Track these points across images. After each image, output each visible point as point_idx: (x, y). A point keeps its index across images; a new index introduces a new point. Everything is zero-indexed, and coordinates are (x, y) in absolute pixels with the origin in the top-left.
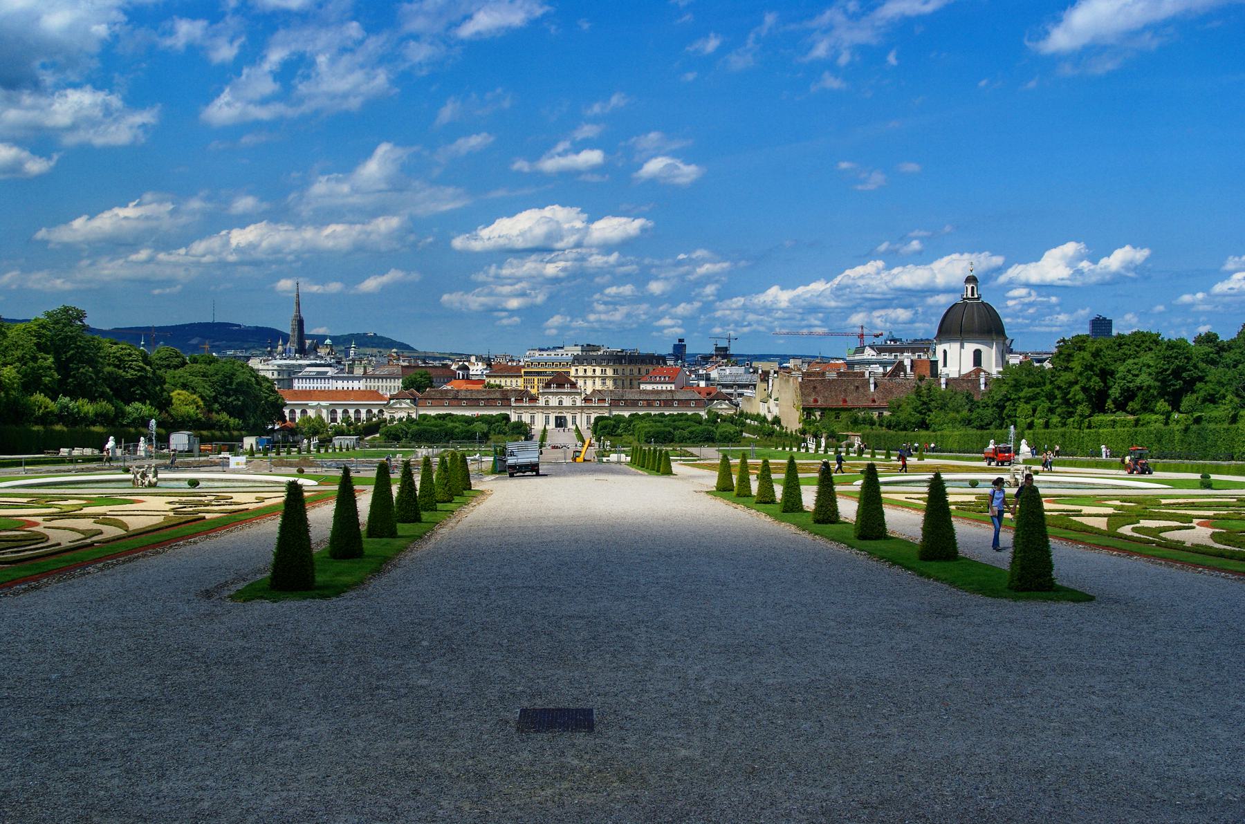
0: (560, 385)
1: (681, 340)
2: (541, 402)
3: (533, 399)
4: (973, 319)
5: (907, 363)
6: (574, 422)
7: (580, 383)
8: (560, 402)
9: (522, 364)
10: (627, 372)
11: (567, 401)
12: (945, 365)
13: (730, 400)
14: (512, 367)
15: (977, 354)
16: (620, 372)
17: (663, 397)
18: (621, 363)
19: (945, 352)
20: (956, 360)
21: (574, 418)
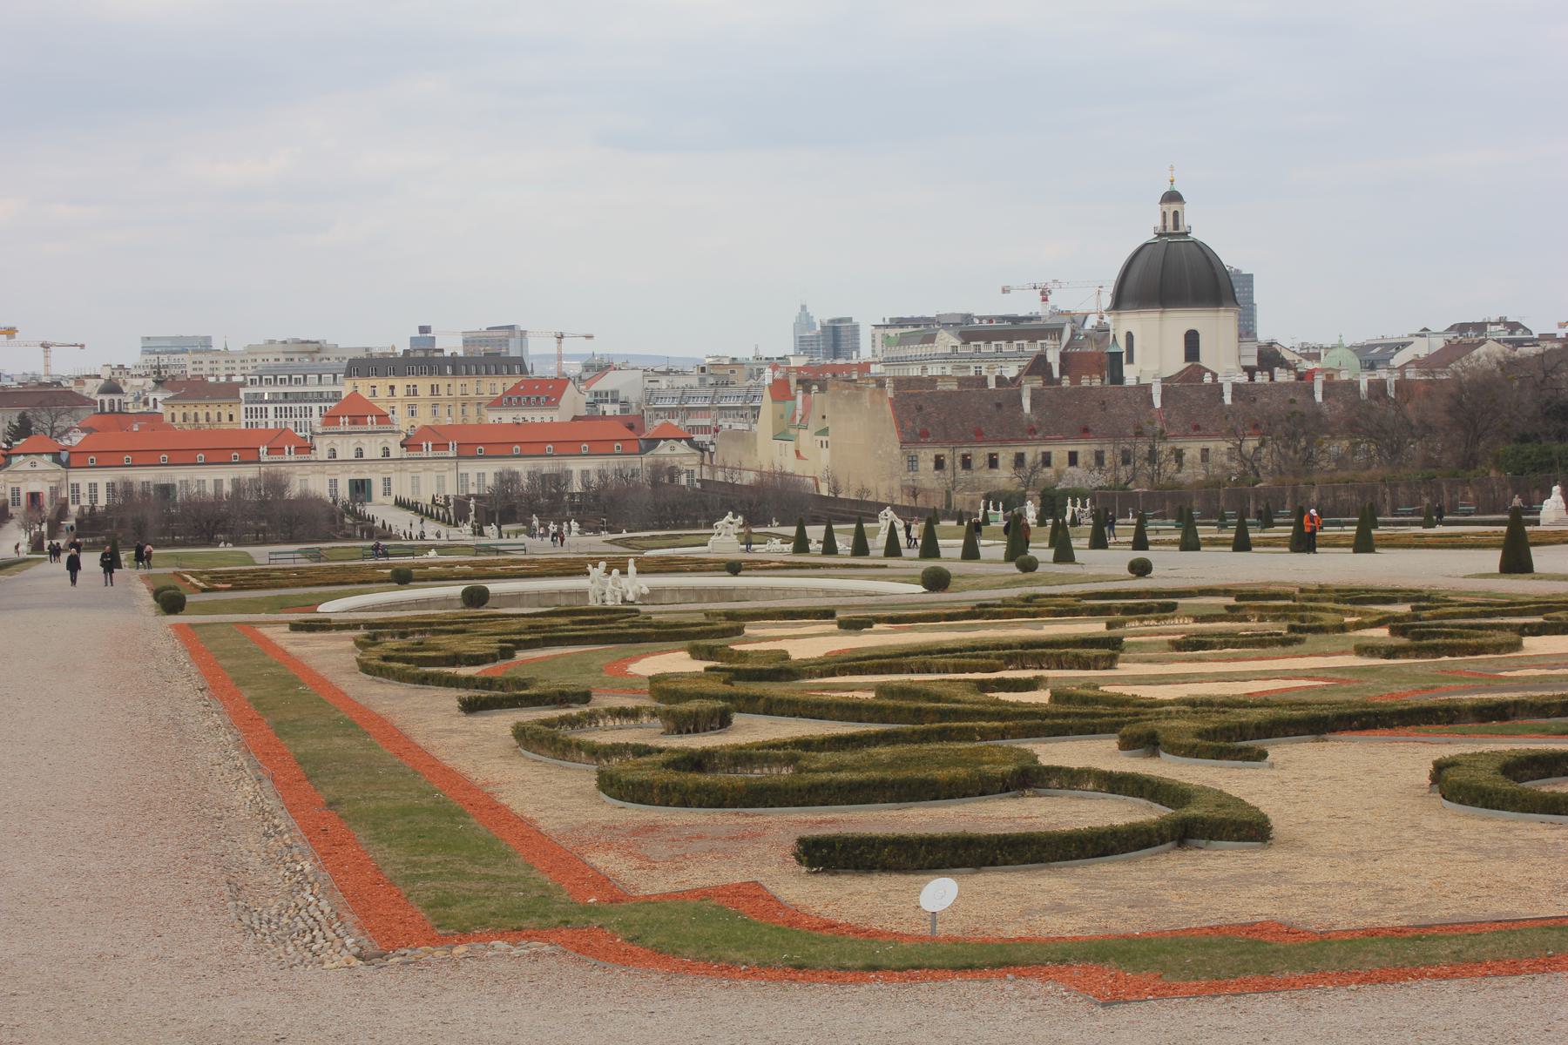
0: (355, 420)
1: (424, 329)
2: (322, 452)
3: (306, 448)
4: (1179, 274)
5: (1053, 358)
6: (387, 492)
8: (360, 453)
9: (237, 379)
11: (373, 448)
12: (1130, 360)
13: (690, 440)
15: (1192, 339)
16: (443, 391)
18: (442, 373)
19: (1130, 336)
20: (1154, 345)
21: (387, 482)
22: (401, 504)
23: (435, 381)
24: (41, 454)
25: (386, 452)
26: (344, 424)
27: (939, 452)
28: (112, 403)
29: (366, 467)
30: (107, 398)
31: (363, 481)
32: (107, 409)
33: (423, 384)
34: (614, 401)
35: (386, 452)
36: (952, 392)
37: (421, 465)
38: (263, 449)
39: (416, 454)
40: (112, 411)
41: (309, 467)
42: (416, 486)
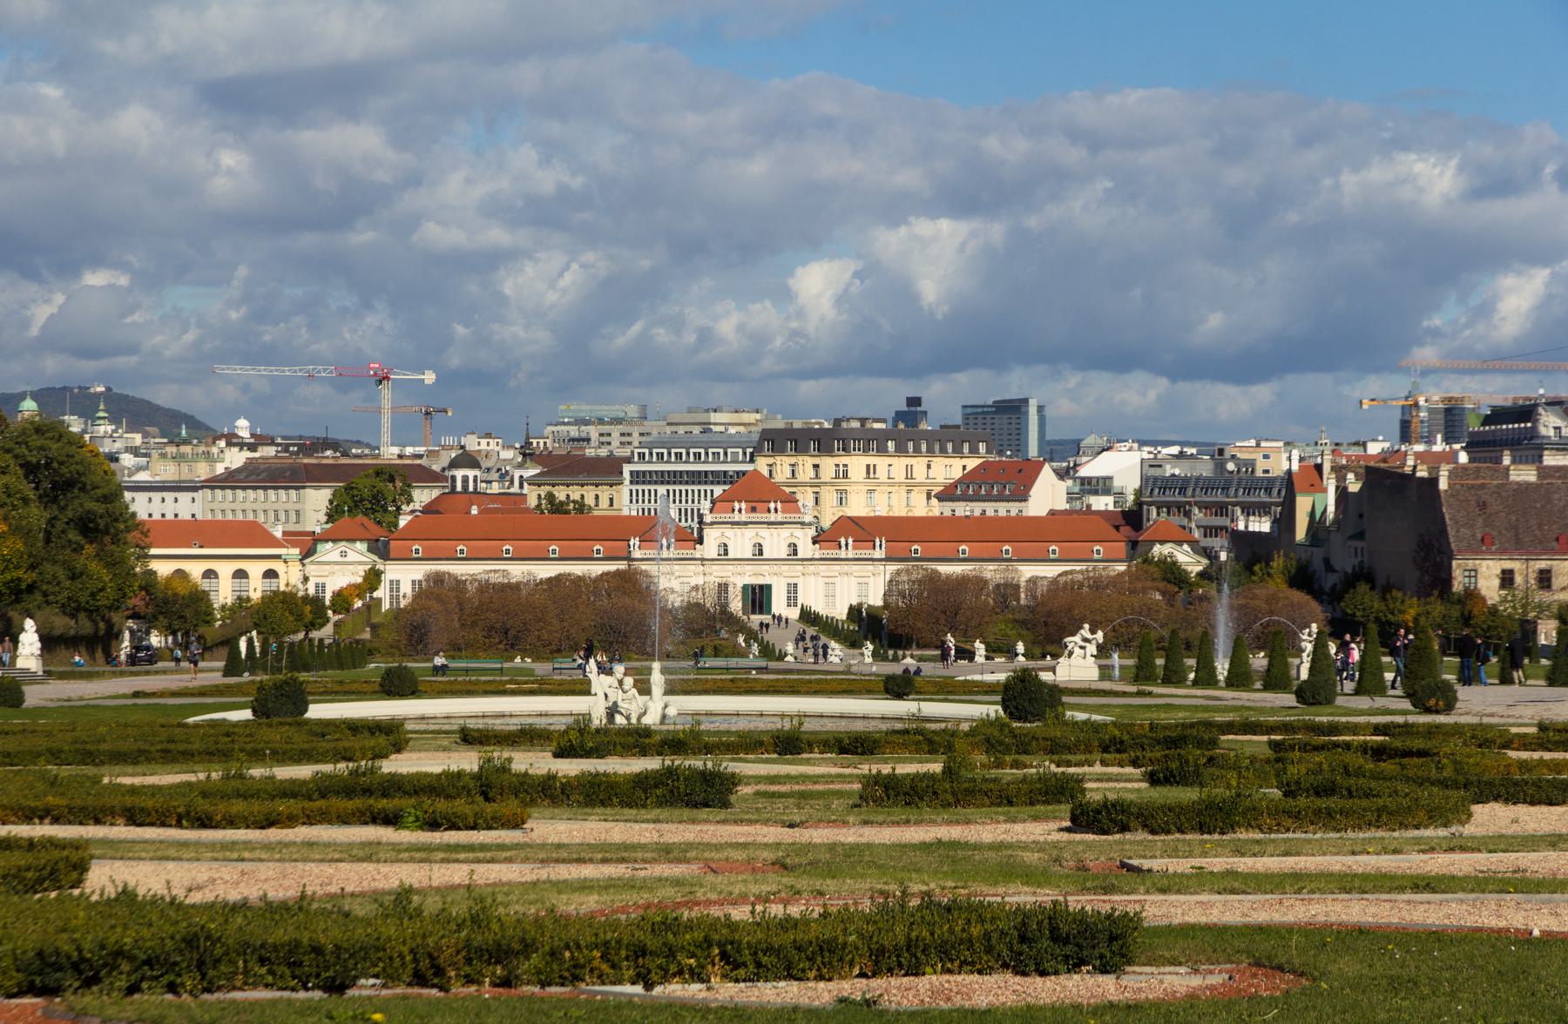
2: (710, 548)
6: (792, 600)
7: (805, 498)
10: (899, 473)
11: (776, 542)
14: (598, 459)
16: (882, 473)
18: (882, 451)
21: (793, 590)
24: (353, 540)
25: (794, 549)
26: (741, 511)
27: (1508, 565)
28: (465, 479)
29: (765, 568)
30: (459, 474)
31: (761, 587)
32: (459, 488)
33: (857, 464)
34: (1107, 491)
35: (794, 549)
36: (1528, 484)
37: (836, 568)
38: (634, 541)
39: (833, 553)
40: (465, 487)
42: (830, 596)
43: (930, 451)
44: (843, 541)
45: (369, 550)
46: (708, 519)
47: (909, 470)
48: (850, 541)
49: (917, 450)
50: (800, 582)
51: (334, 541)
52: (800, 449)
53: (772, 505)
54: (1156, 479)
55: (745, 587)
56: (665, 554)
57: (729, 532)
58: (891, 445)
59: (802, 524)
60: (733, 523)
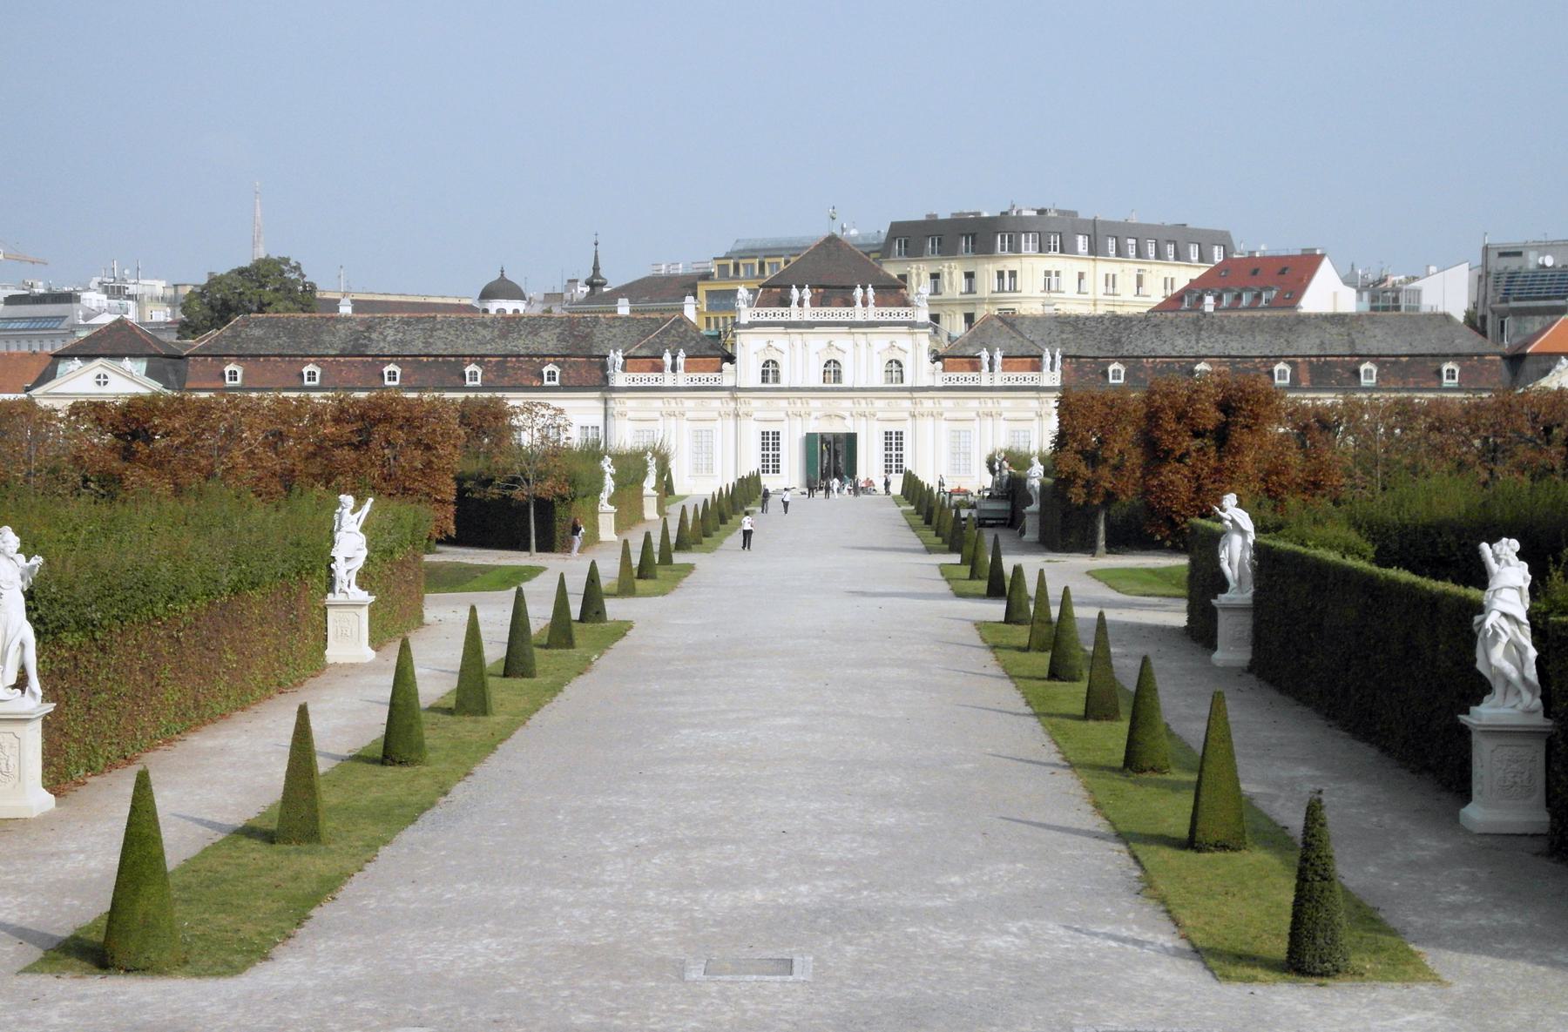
0: (834, 292)
2: (746, 370)
6: (893, 462)
8: (833, 369)
11: (864, 358)
16: (1068, 283)
17: (1307, 345)
18: (1066, 248)
21: (894, 441)
22: (914, 490)
23: (1053, 262)
26: (802, 306)
29: (845, 405)
37: (973, 404)
38: (616, 357)
39: (965, 377)
41: (717, 404)
43: (1140, 254)
44: (985, 355)
45: (150, 373)
46: (746, 315)
47: (1111, 280)
48: (998, 358)
49: (1120, 252)
50: (906, 428)
51: (88, 357)
52: (947, 250)
53: (859, 292)
54: (1512, 276)
55: (810, 439)
56: (668, 379)
57: (780, 340)
58: (1082, 242)
59: (912, 325)
60: (788, 325)
